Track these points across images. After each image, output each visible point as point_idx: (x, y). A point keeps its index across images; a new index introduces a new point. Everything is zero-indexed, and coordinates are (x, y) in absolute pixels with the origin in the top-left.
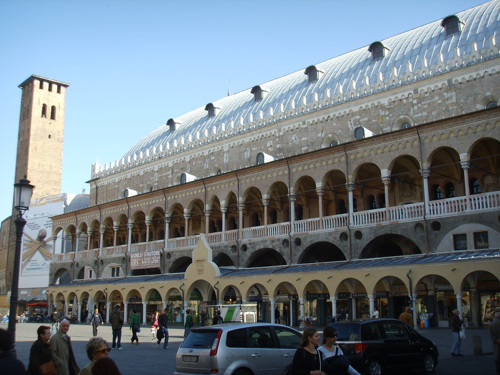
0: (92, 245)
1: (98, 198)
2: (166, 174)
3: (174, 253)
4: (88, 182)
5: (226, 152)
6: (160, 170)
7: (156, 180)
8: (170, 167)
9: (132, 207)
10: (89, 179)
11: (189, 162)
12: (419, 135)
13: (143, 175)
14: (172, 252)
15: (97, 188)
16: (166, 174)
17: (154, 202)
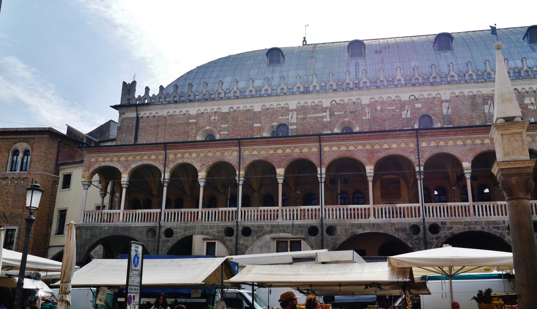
0: (378, 194)
1: (140, 133)
2: (315, 115)
3: (448, 225)
4: (115, 107)
5: (446, 101)
6: (302, 110)
7: (294, 120)
8: (327, 108)
9: (326, 149)
10: (119, 103)
11: (369, 105)
12: (417, 138)
13: (260, 112)
14: (443, 223)
15: (138, 118)
16: (315, 115)
17: (386, 146)
